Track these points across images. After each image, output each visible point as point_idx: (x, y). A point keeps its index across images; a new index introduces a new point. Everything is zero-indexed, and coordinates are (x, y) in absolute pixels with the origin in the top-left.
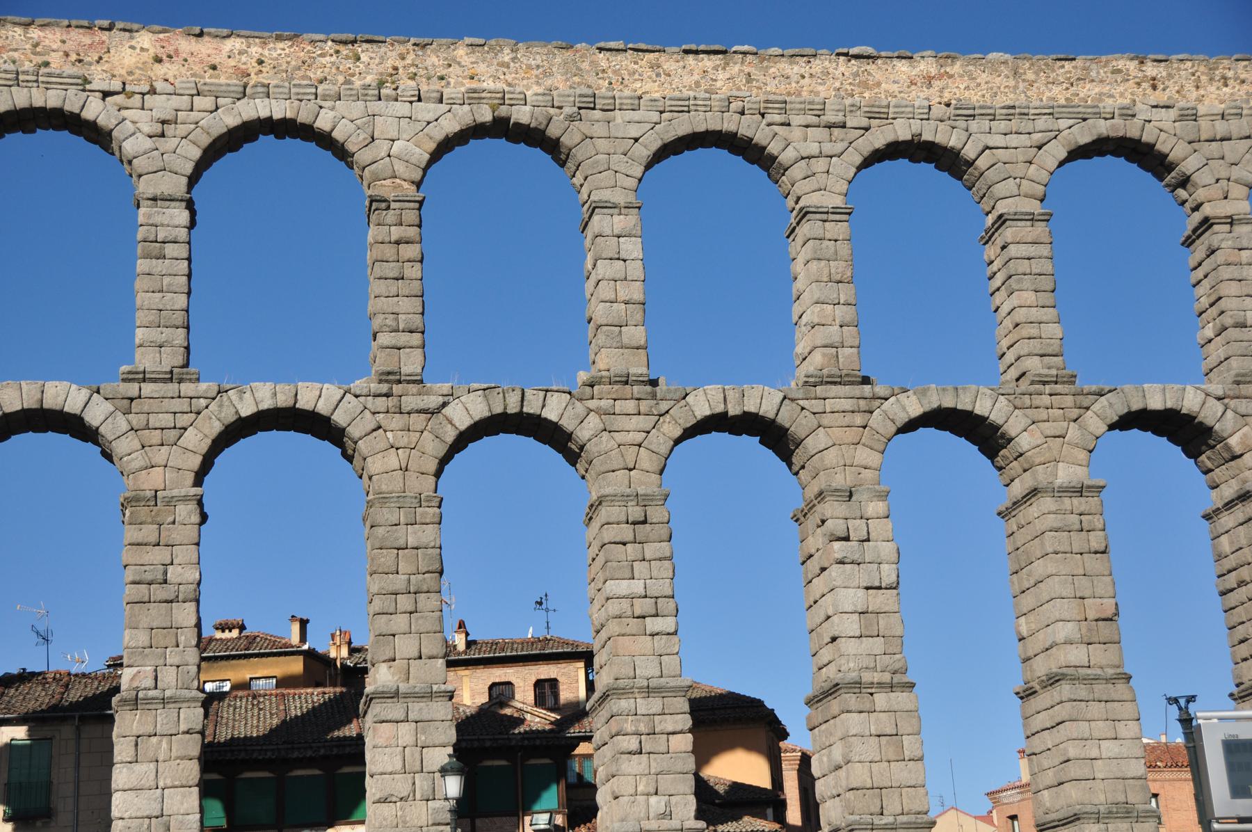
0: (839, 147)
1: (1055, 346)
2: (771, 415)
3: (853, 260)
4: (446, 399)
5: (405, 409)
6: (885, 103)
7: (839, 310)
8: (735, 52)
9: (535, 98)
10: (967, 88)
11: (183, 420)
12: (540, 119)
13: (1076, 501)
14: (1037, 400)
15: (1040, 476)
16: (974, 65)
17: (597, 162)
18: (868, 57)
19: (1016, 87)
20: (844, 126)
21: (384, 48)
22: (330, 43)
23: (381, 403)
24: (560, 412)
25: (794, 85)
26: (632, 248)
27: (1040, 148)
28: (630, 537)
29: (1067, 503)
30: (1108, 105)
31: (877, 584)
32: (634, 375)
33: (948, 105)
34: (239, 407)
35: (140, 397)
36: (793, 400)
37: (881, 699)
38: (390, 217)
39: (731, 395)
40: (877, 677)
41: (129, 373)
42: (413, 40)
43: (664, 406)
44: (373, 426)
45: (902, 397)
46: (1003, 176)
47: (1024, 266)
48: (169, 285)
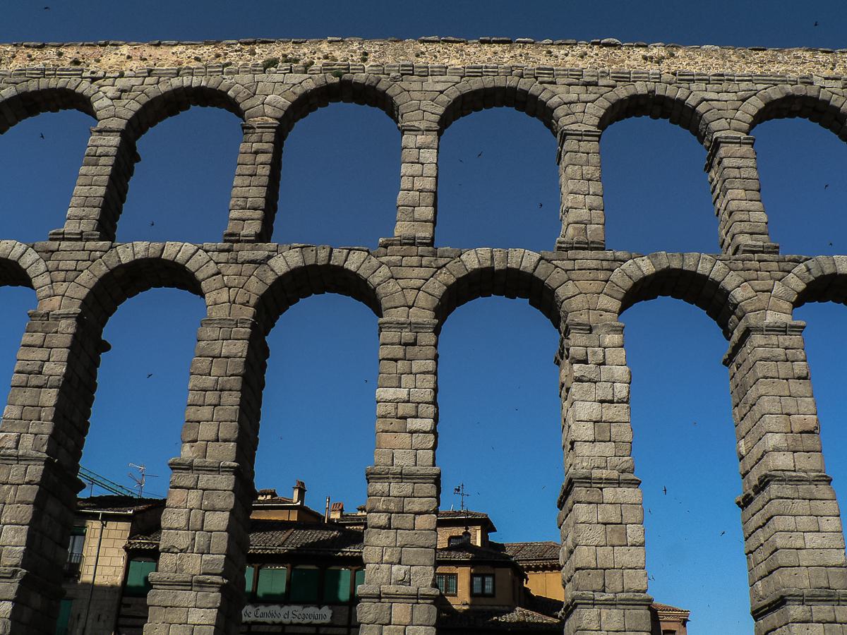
0: (593, 97)
1: (762, 227)
2: (529, 270)
3: (602, 166)
5: (240, 260)
7: (589, 199)
8: (518, 42)
9: (371, 68)
11: (82, 265)
12: (372, 80)
13: (781, 338)
14: (748, 264)
15: (752, 319)
18: (615, 45)
19: (724, 65)
20: (596, 84)
21: (273, 46)
22: (239, 45)
24: (359, 264)
25: (560, 61)
26: (430, 156)
27: (744, 100)
28: (401, 355)
29: (774, 339)
30: (793, 76)
31: (610, 398)
32: (419, 238)
33: (674, 74)
34: (122, 257)
35: (58, 250)
36: (549, 261)
37: (609, 493)
38: (254, 137)
39: (498, 254)
40: (605, 474)
41: (54, 234)
43: (441, 262)
44: (214, 271)
45: (638, 260)
46: (716, 117)
47: (735, 173)
48: (96, 180)
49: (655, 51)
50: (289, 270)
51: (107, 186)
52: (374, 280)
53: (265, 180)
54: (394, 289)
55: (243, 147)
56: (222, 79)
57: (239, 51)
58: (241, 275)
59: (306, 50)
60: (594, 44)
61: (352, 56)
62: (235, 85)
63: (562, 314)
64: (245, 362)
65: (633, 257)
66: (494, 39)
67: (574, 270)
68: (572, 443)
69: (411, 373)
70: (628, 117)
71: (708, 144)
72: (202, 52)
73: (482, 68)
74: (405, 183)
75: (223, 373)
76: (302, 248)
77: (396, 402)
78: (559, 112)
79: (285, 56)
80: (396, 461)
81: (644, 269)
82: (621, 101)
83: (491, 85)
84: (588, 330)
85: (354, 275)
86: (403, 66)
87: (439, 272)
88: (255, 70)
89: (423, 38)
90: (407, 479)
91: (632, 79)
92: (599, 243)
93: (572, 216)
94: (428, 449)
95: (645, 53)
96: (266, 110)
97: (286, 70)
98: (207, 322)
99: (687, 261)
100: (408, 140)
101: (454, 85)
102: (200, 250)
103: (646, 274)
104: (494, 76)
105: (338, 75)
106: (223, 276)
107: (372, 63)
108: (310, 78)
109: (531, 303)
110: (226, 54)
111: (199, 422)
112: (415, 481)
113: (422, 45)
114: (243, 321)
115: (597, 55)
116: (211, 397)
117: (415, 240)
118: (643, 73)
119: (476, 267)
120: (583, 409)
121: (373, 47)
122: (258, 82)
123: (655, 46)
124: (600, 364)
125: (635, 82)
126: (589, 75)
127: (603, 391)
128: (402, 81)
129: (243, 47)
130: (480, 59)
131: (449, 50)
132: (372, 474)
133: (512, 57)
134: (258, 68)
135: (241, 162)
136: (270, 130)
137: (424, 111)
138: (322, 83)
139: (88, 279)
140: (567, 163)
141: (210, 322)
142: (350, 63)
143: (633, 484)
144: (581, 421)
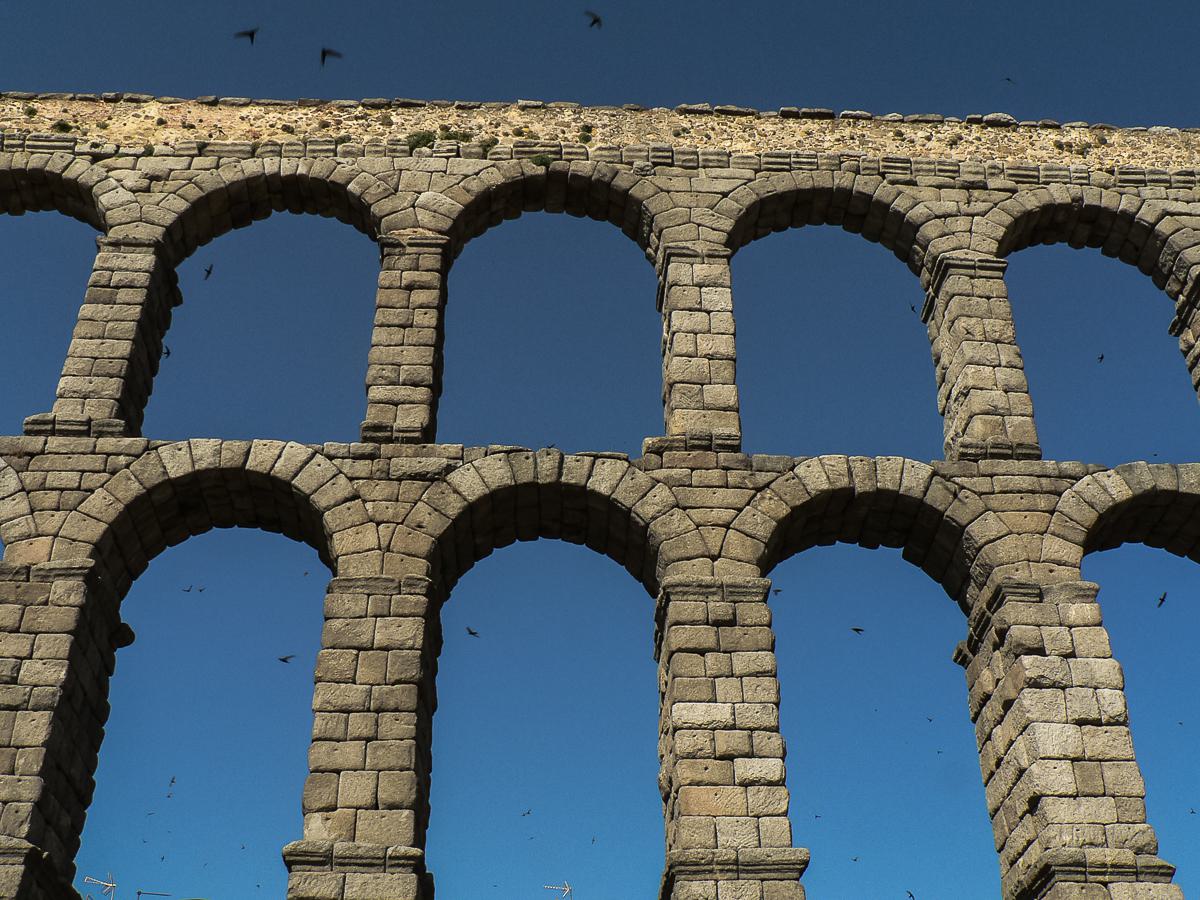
0: (981, 207)
2: (917, 493)
3: (1016, 318)
4: (452, 462)
5: (395, 474)
6: (1033, 165)
7: (1002, 374)
9: (599, 152)
10: (1131, 156)
11: (90, 480)
12: (604, 171)
16: (1137, 135)
17: (676, 213)
19: (1191, 158)
20: (985, 187)
22: (360, 108)
23: (363, 468)
25: (919, 148)
26: (720, 299)
28: (710, 642)
31: (1094, 715)
32: (719, 437)
33: (1111, 172)
34: (169, 466)
35: (42, 452)
36: (948, 478)
38: (404, 261)
40: (1110, 855)
41: (35, 422)
42: (457, 103)
43: (762, 478)
45: (1100, 476)
48: (113, 329)
49: (1074, 134)
50: (487, 491)
51: (133, 340)
52: (646, 510)
53: (429, 335)
54: (682, 527)
55: (385, 278)
56: (334, 164)
57: (362, 118)
58: (397, 500)
59: (481, 121)
60: (972, 121)
61: (564, 132)
62: (361, 174)
63: (975, 570)
64: (421, 656)
65: (1091, 470)
66: (804, 110)
67: (993, 493)
68: (1034, 803)
69: (732, 676)
70: (1033, 243)
71: (1176, 288)
72: (294, 118)
73: (789, 156)
74: (682, 344)
75: (379, 677)
76: (508, 452)
77: (713, 727)
78: (930, 230)
79: (445, 128)
80: (721, 839)
81: (1114, 492)
82: (1028, 215)
83: (808, 185)
84: (1037, 595)
85: (608, 503)
86: (655, 149)
87: (759, 495)
88: (394, 151)
89: (684, 106)
90: (748, 872)
91: (1042, 180)
92: (1031, 447)
93: (977, 401)
94: (779, 815)
95: (1058, 138)
96: (419, 218)
97: (449, 151)
98: (342, 584)
99: (1185, 477)
100: (678, 270)
101: (745, 184)
102: (318, 456)
103: (1118, 500)
104: (811, 170)
105: (544, 162)
106: (365, 501)
107: (599, 145)
108: (493, 166)
109: (906, 556)
110: (339, 122)
111: (338, 772)
112: (762, 876)
113: (682, 117)
114: (411, 583)
115: (979, 139)
116: (359, 724)
117: (711, 440)
118: (1060, 170)
119: (825, 486)
120: (1050, 734)
121: (600, 118)
122: (401, 170)
123: (1073, 127)
124: (1066, 656)
125: (1048, 183)
126: (970, 172)
127: (1080, 703)
128: (655, 174)
129: (368, 112)
130: (784, 142)
131: (730, 127)
132: (682, 864)
133: (838, 140)
134: (399, 148)
135: (383, 304)
136: (433, 250)
137: (699, 225)
138: (515, 174)
139: (104, 504)
140: (954, 314)
141: (349, 584)
142: (562, 143)
143: (1163, 874)
144: (1049, 758)
